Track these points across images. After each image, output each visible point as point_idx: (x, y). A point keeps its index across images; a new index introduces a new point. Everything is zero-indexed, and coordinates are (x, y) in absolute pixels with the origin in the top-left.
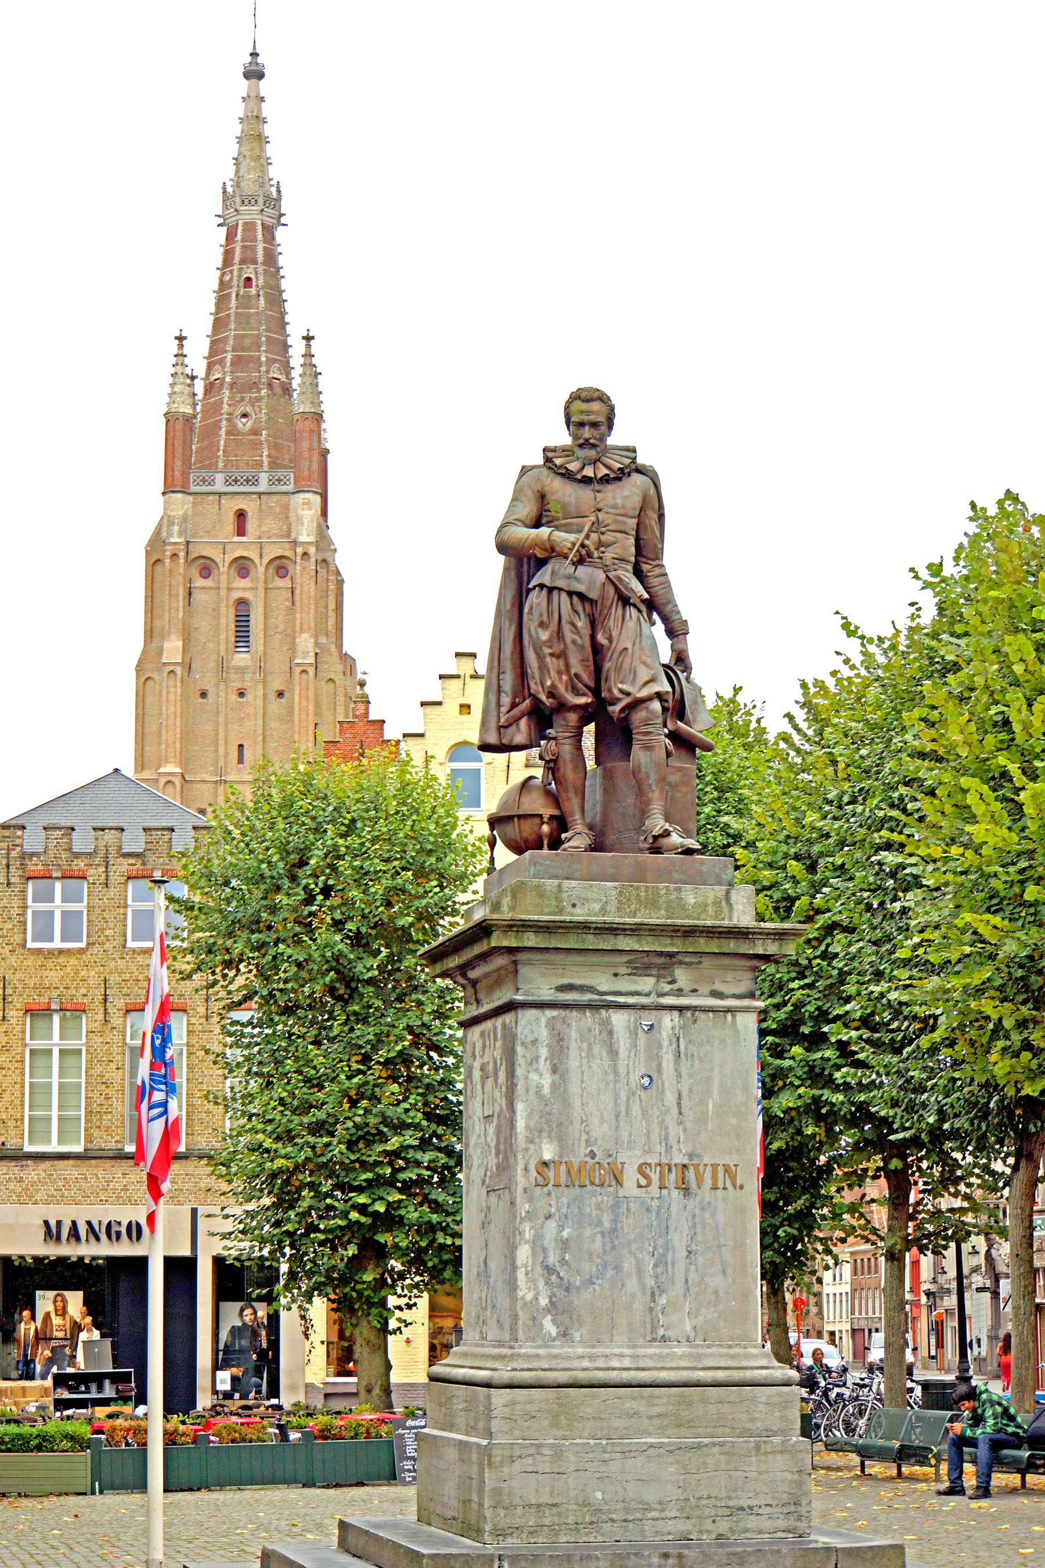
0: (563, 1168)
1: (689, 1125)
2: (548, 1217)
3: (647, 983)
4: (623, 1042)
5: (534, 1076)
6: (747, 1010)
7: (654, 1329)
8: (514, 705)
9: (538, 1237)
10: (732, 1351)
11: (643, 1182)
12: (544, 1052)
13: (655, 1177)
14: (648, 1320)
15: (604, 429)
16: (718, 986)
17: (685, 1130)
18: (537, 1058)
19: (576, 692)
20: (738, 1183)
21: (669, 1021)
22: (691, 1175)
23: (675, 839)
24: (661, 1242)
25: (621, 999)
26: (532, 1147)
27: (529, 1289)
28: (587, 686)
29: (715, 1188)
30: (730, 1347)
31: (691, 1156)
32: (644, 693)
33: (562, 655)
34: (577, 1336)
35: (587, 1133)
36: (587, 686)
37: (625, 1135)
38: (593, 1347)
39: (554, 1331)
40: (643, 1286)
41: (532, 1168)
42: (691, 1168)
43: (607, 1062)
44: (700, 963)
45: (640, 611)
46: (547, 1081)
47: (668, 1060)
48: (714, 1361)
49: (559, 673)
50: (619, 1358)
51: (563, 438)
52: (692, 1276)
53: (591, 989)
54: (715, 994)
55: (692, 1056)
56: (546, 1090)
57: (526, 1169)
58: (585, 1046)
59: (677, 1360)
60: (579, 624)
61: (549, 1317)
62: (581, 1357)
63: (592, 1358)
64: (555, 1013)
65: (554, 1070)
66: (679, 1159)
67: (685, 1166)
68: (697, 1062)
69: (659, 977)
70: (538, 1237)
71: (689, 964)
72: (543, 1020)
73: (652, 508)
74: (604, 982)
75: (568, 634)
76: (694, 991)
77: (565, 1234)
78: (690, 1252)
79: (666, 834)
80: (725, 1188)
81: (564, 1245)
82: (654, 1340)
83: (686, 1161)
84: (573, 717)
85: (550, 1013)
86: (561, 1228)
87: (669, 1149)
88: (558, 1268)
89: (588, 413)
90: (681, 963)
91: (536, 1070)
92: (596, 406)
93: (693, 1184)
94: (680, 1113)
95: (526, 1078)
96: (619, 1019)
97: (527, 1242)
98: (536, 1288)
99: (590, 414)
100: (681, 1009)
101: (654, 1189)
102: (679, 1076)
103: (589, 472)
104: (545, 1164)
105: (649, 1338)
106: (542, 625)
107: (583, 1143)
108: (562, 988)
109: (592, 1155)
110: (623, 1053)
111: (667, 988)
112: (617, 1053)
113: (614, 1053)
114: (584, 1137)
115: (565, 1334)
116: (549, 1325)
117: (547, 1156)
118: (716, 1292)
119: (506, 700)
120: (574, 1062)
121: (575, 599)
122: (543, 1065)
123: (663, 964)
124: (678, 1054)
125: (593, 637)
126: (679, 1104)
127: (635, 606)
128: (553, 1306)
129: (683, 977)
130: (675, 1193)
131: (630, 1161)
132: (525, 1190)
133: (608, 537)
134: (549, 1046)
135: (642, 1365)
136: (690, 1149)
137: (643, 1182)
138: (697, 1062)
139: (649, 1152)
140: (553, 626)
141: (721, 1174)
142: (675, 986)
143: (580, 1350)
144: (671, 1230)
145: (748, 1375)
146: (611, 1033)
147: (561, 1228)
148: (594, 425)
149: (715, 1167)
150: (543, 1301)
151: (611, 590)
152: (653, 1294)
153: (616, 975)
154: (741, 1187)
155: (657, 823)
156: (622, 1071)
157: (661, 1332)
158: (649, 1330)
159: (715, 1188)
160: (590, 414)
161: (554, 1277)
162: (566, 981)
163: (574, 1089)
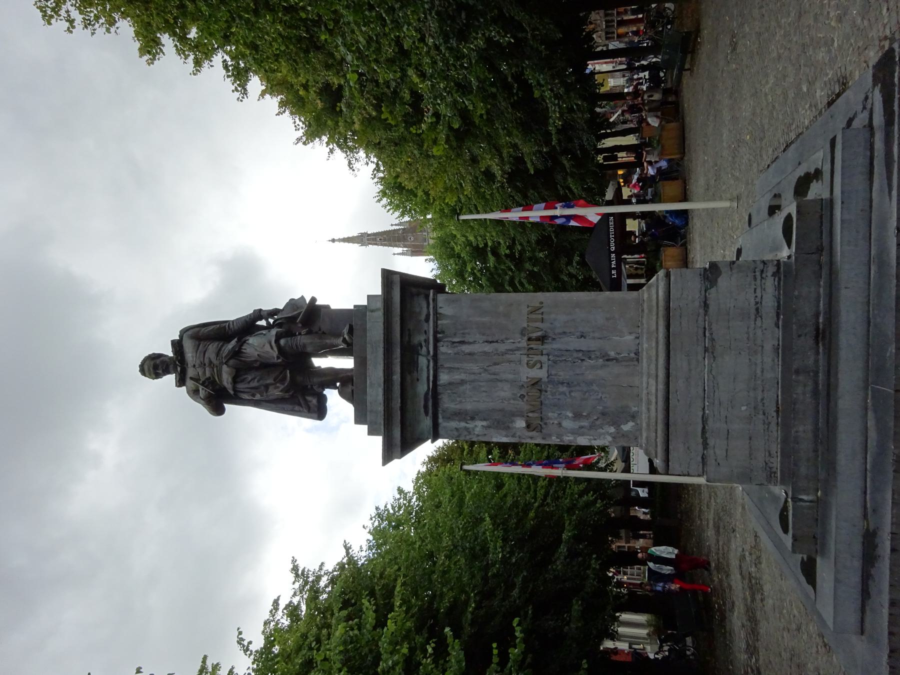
0: (530, 415)
1: (503, 337)
2: (560, 424)
3: (423, 361)
4: (457, 377)
5: (478, 430)
6: (434, 300)
7: (632, 360)
8: (300, 404)
9: (574, 432)
10: (646, 311)
11: (538, 365)
12: (463, 424)
13: (536, 358)
14: (625, 363)
15: (158, 361)
16: (423, 317)
17: (507, 339)
18: (466, 429)
19: (285, 378)
20: (538, 305)
21: (443, 349)
22: (534, 335)
24: (575, 355)
25: (431, 378)
26: (518, 434)
27: (604, 438)
28: (281, 373)
29: (542, 320)
30: (643, 311)
31: (522, 333)
32: (275, 349)
33: (267, 387)
34: (635, 409)
35: (509, 399)
36: (281, 373)
37: (511, 377)
38: (642, 400)
39: (631, 424)
40: (602, 366)
41: (531, 434)
42: (531, 335)
43: (468, 386)
44: (409, 330)
45: (245, 342)
46: (480, 424)
47: (466, 348)
48: (653, 323)
49: (277, 388)
50: (648, 385)
52: (597, 335)
53: (427, 394)
54: (427, 320)
55: (463, 334)
56: (485, 423)
57: (531, 438)
58: (458, 399)
59: (652, 350)
60: (250, 378)
61: (622, 426)
62: (649, 410)
63: (649, 403)
64: (440, 416)
65: (473, 419)
66: (524, 343)
67: (529, 339)
68: (466, 331)
69: (419, 354)
70: (574, 432)
71: (410, 336)
72: (445, 424)
73: (199, 332)
74: (422, 388)
75: (254, 384)
76: (425, 332)
77: (570, 415)
78: (582, 336)
79: (344, 340)
80: (542, 313)
81: (577, 416)
82: (638, 360)
83: (526, 338)
84: (299, 379)
85: (440, 420)
86: (567, 417)
87: (518, 349)
88: (592, 420)
89: (149, 370)
90: (409, 341)
91: (473, 429)
92: (146, 367)
93: (539, 334)
94: (497, 342)
95: (478, 436)
96: (444, 378)
97: (575, 439)
98: (604, 434)
99: (154, 366)
100: (436, 341)
101: (544, 359)
102: (474, 342)
103: (179, 369)
104: (528, 426)
105: (636, 363)
106: (254, 395)
107: (516, 402)
108: (427, 413)
109: (522, 397)
110: (463, 376)
111: (424, 349)
112: (462, 380)
113: (463, 382)
114: (512, 402)
115: (633, 417)
116: (627, 427)
117: (524, 424)
118: (608, 319)
119: (297, 408)
120: (469, 407)
121: (238, 380)
122: (470, 425)
123: (410, 353)
124: (462, 342)
125: (257, 369)
126: (491, 342)
127: (242, 345)
128: (616, 424)
129: (419, 338)
130: (546, 346)
131: (527, 374)
132: (544, 439)
133: (207, 361)
134: (460, 421)
135: (653, 372)
136: (518, 335)
137: (538, 365)
138: (466, 331)
139: (520, 361)
140: (253, 391)
141: (533, 316)
142: (423, 344)
143: (644, 408)
144: (569, 348)
145: (662, 303)
146: (450, 384)
147: (567, 417)
148: (156, 367)
149: (529, 320)
150: (612, 430)
151: (231, 362)
152: (608, 360)
153: (418, 380)
154: (542, 303)
156: (472, 377)
157: (632, 355)
158: (631, 363)
159: (542, 320)
160: (154, 366)
161: (598, 423)
162: (422, 410)
163: (482, 406)
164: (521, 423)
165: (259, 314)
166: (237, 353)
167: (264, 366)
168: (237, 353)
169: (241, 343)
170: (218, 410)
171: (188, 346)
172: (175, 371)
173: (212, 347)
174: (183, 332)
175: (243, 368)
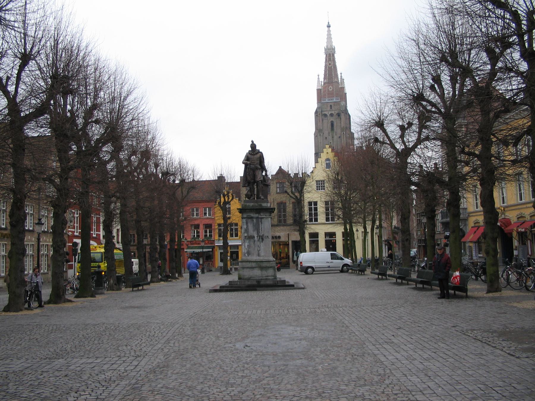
3: (257, 215)
23: (262, 197)
51: (250, 149)
74: (252, 215)
99: (253, 146)
115: (248, 256)
120: (249, 224)
155: (261, 195)
160: (253, 146)
164: (246, 235)
165: (266, 171)
166: (257, 169)
167: (254, 176)
168: (257, 169)
169: (259, 169)
170: (243, 163)
171: (258, 155)
172: (252, 150)
173: (258, 162)
174: (261, 153)
175: (254, 170)
